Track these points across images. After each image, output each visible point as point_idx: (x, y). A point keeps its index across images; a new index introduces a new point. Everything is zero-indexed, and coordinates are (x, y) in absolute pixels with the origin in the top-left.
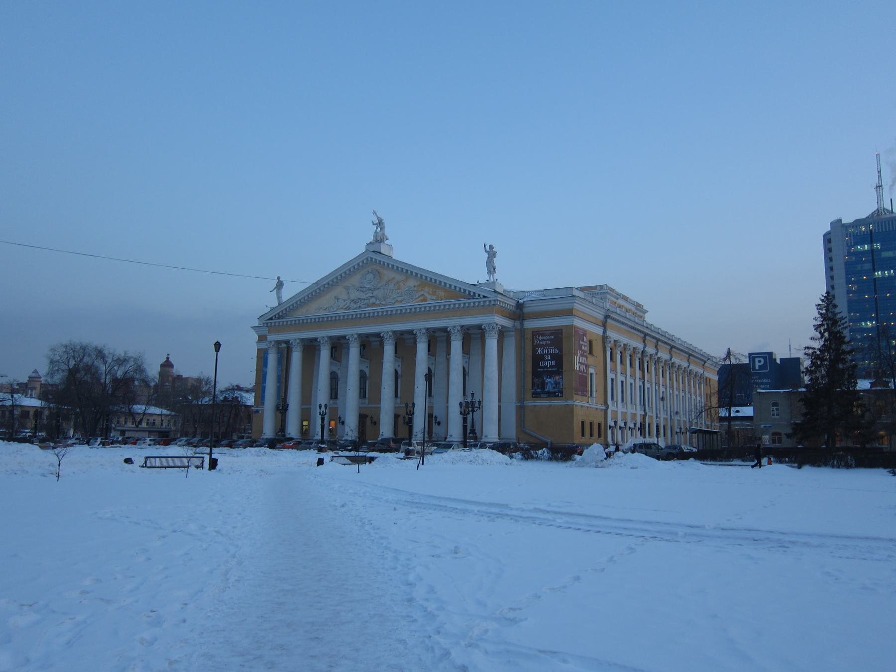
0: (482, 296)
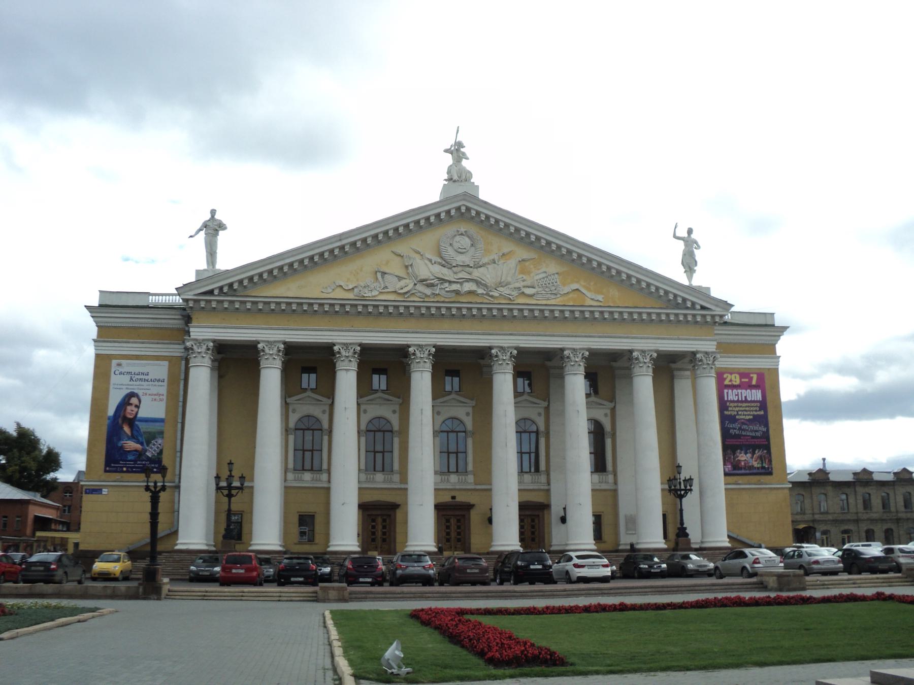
0: (698, 307)
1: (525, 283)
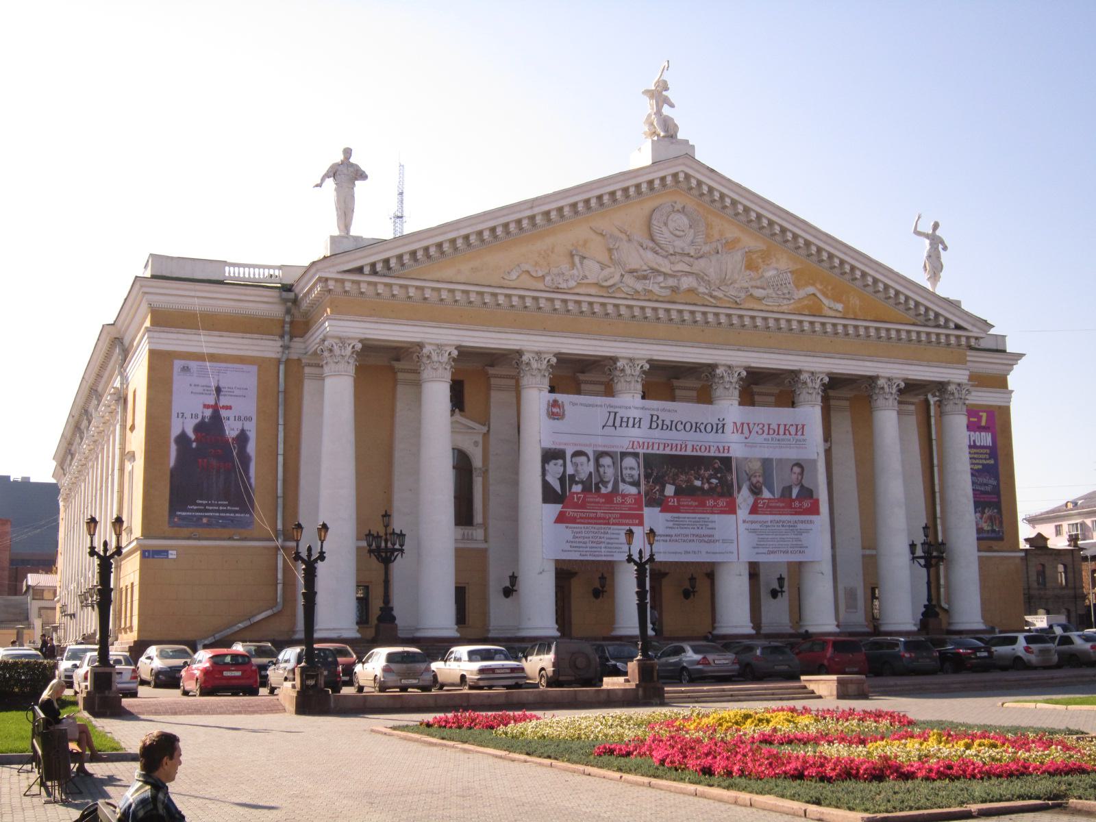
0: (952, 325)
1: (753, 283)
